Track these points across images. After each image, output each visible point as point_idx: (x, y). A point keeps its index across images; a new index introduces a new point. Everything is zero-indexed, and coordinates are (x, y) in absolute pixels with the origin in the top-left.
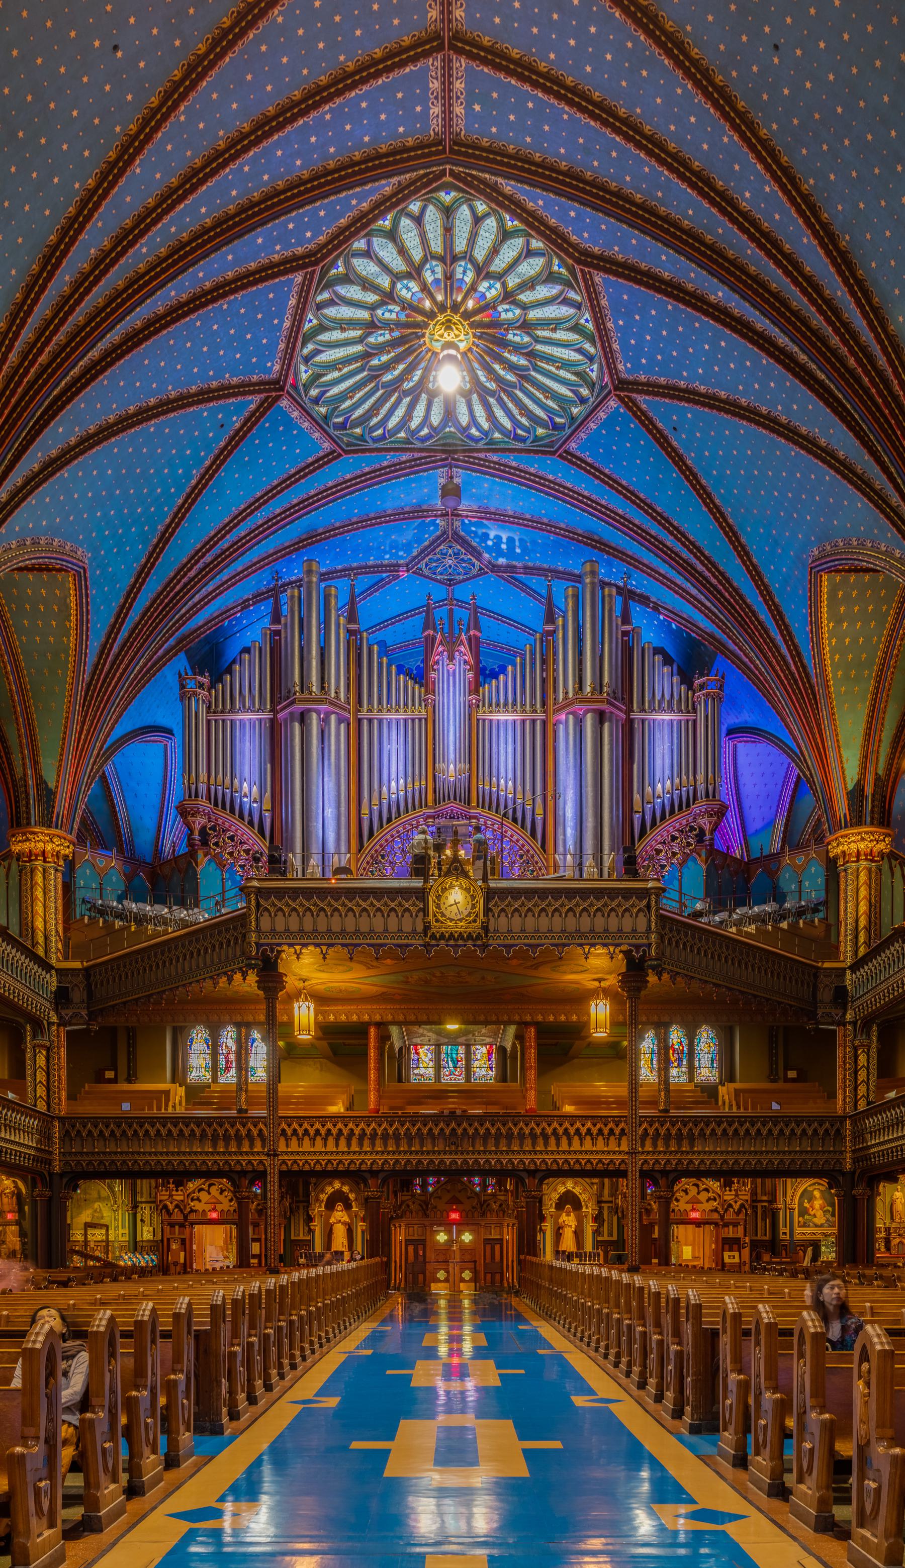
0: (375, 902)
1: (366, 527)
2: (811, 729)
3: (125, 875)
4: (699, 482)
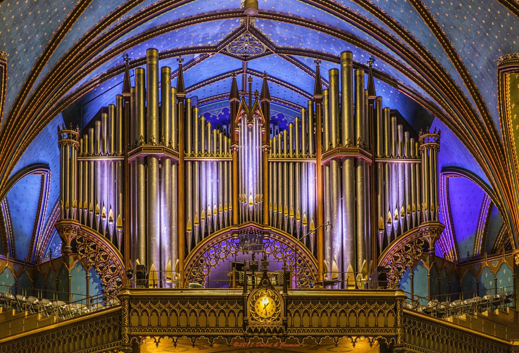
0: (210, 306)
1: (190, 24)
2: (501, 174)
3: (15, 273)
4: (422, 7)
